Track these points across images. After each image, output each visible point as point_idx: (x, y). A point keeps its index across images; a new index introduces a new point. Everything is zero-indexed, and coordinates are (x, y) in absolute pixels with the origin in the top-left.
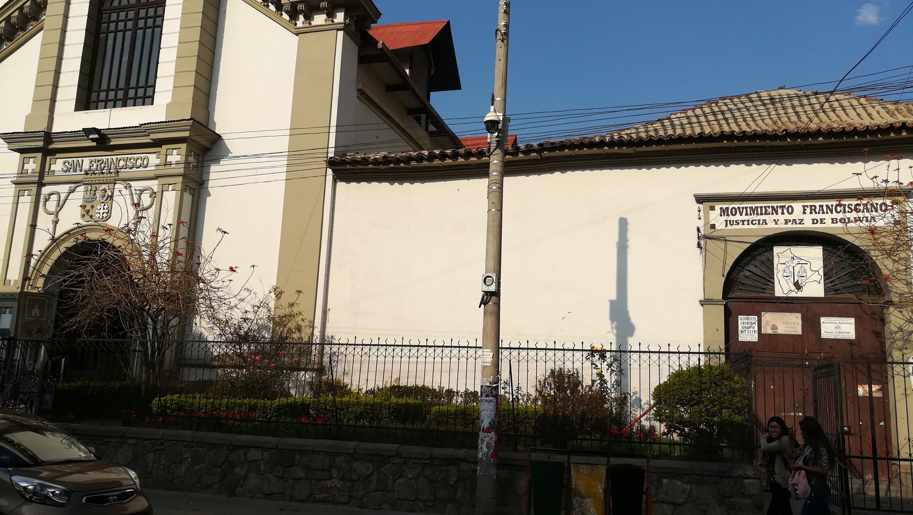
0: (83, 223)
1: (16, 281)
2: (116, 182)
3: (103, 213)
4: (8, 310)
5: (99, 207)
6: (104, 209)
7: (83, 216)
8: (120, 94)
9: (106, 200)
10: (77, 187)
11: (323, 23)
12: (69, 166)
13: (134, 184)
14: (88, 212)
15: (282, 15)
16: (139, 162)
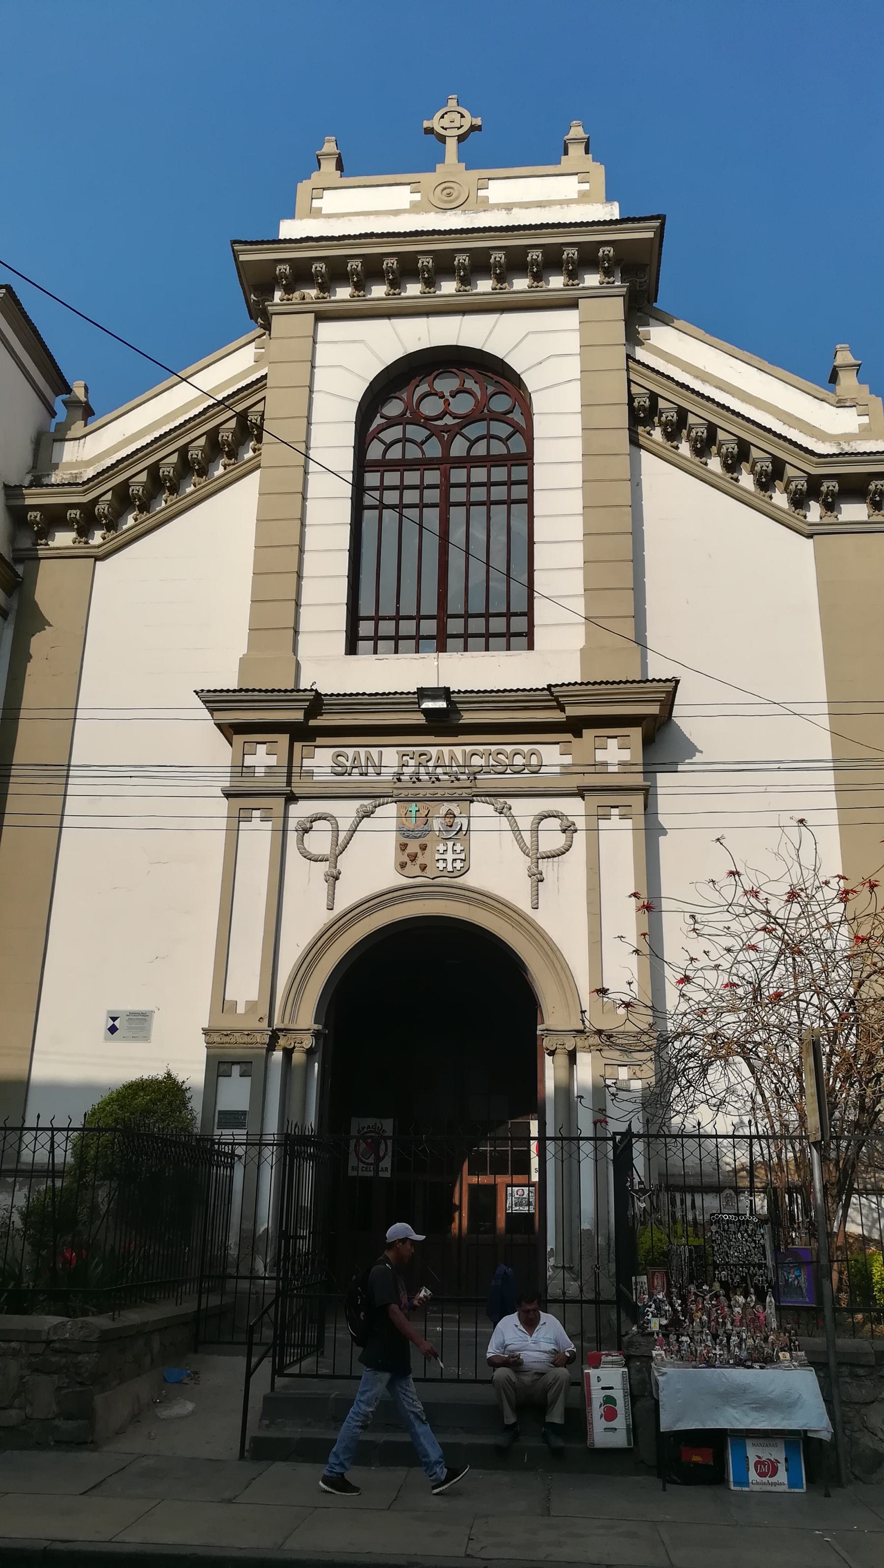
0: (405, 881)
1: (251, 1006)
2: (475, 798)
3: (455, 860)
4: (236, 1069)
5: (441, 848)
6: (454, 851)
7: (403, 865)
8: (429, 627)
9: (456, 834)
10: (379, 806)
11: (865, 518)
12: (348, 764)
13: (519, 806)
14: (413, 858)
15: (771, 497)
16: (519, 760)
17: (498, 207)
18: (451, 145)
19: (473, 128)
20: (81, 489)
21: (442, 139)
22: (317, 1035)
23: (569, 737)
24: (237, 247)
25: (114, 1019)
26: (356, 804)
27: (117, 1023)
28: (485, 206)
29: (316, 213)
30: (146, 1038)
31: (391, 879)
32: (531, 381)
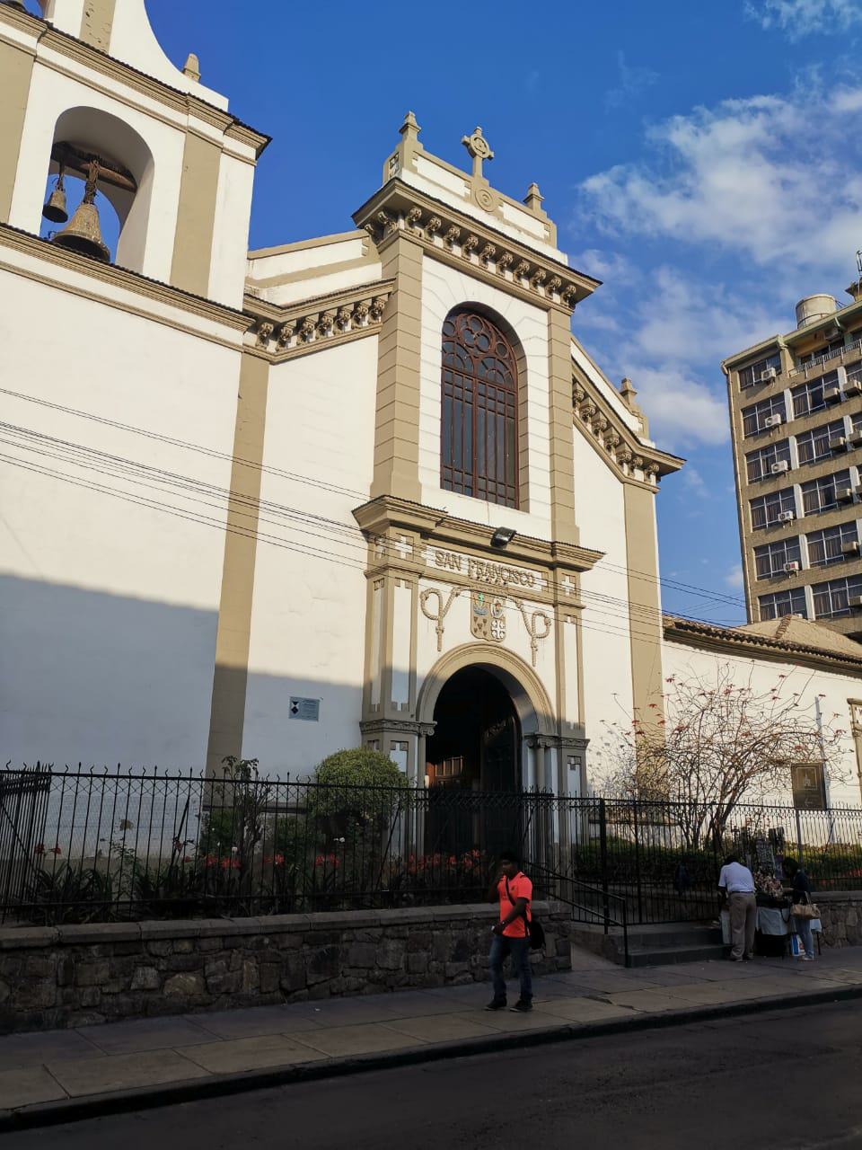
1: (406, 707)
7: (476, 631)
13: (525, 602)
16: (524, 579)
17: (508, 223)
18: (478, 162)
19: (490, 158)
20: (279, 311)
21: (473, 155)
22: (436, 728)
23: (546, 569)
24: (397, 182)
25: (295, 703)
26: (449, 588)
27: (297, 706)
28: (500, 217)
29: (414, 170)
30: (316, 718)
31: (469, 639)
32: (527, 347)
